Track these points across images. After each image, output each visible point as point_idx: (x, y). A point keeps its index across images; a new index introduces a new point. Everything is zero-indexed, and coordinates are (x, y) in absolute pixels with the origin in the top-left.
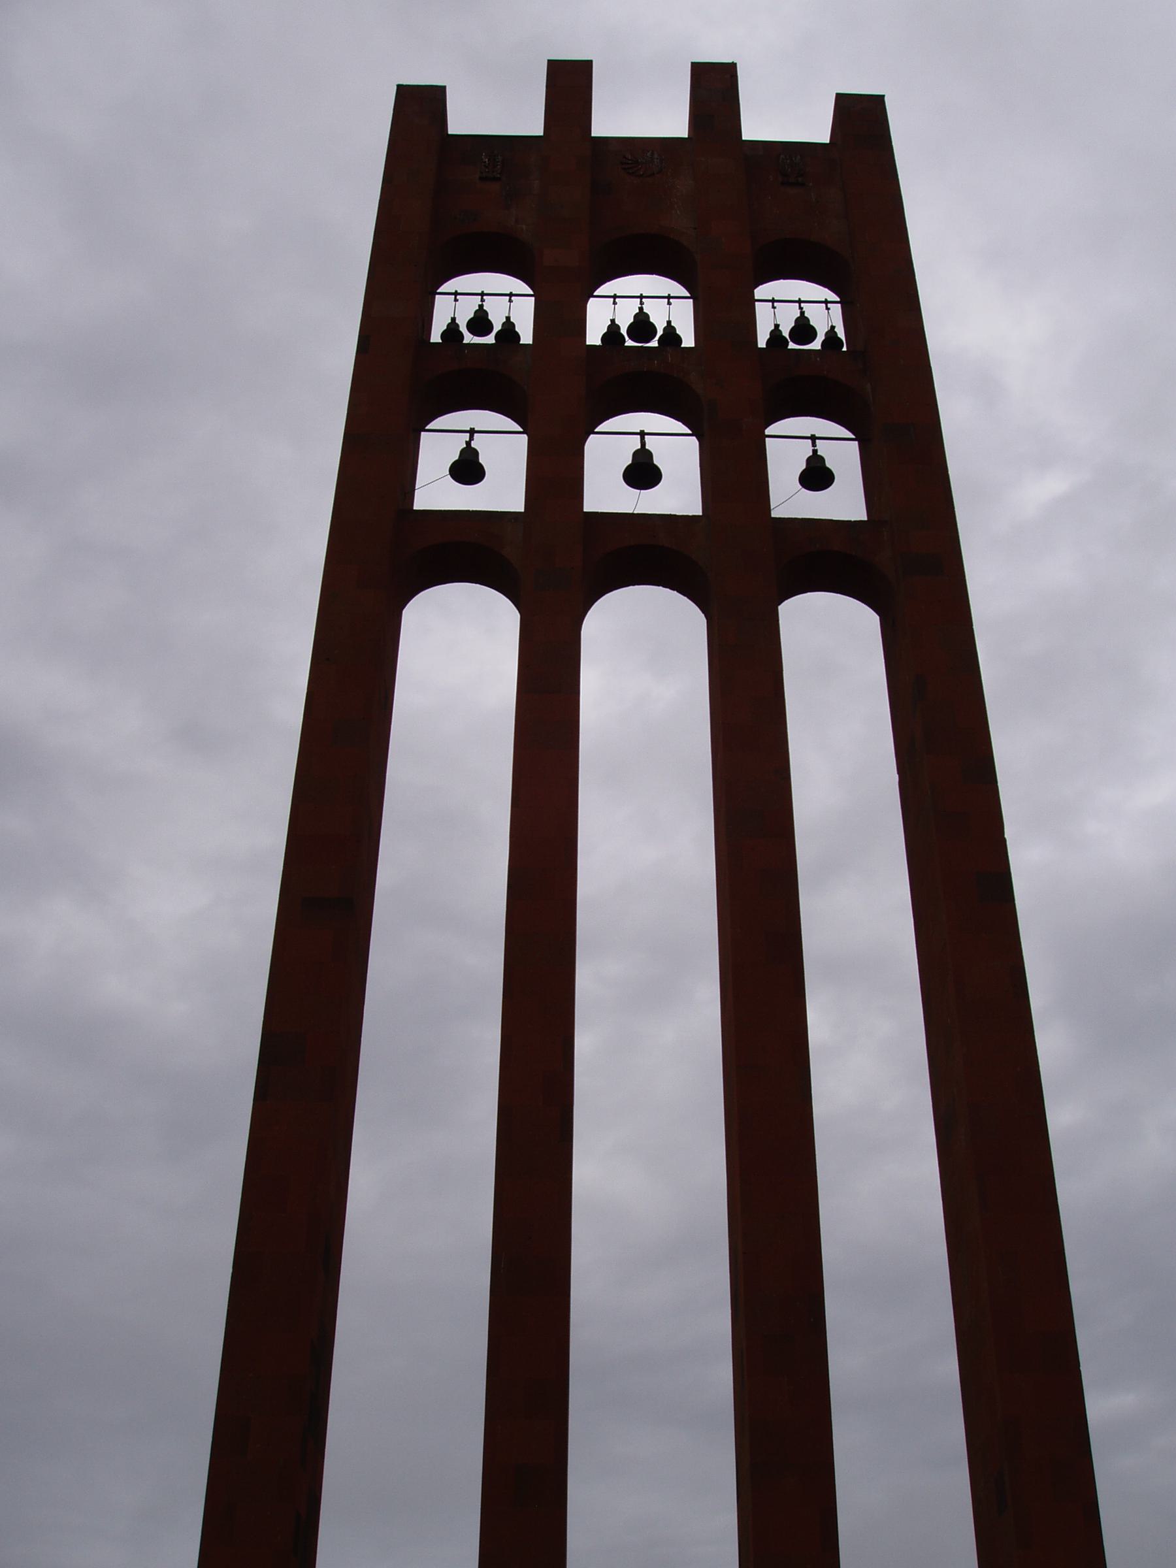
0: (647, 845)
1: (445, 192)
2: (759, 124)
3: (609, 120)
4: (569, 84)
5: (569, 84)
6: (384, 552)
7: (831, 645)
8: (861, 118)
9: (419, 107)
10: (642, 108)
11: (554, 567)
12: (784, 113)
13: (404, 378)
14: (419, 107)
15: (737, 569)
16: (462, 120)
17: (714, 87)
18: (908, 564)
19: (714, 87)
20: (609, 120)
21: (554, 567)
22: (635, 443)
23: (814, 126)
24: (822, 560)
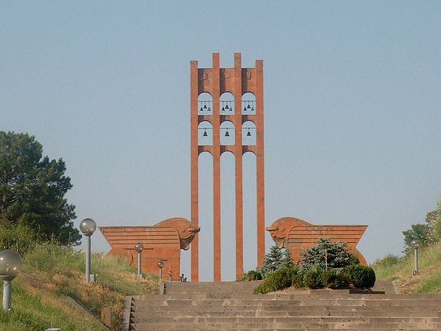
4: (216, 57)
5: (216, 57)
8: (260, 64)
10: (227, 63)
17: (238, 57)
19: (238, 57)
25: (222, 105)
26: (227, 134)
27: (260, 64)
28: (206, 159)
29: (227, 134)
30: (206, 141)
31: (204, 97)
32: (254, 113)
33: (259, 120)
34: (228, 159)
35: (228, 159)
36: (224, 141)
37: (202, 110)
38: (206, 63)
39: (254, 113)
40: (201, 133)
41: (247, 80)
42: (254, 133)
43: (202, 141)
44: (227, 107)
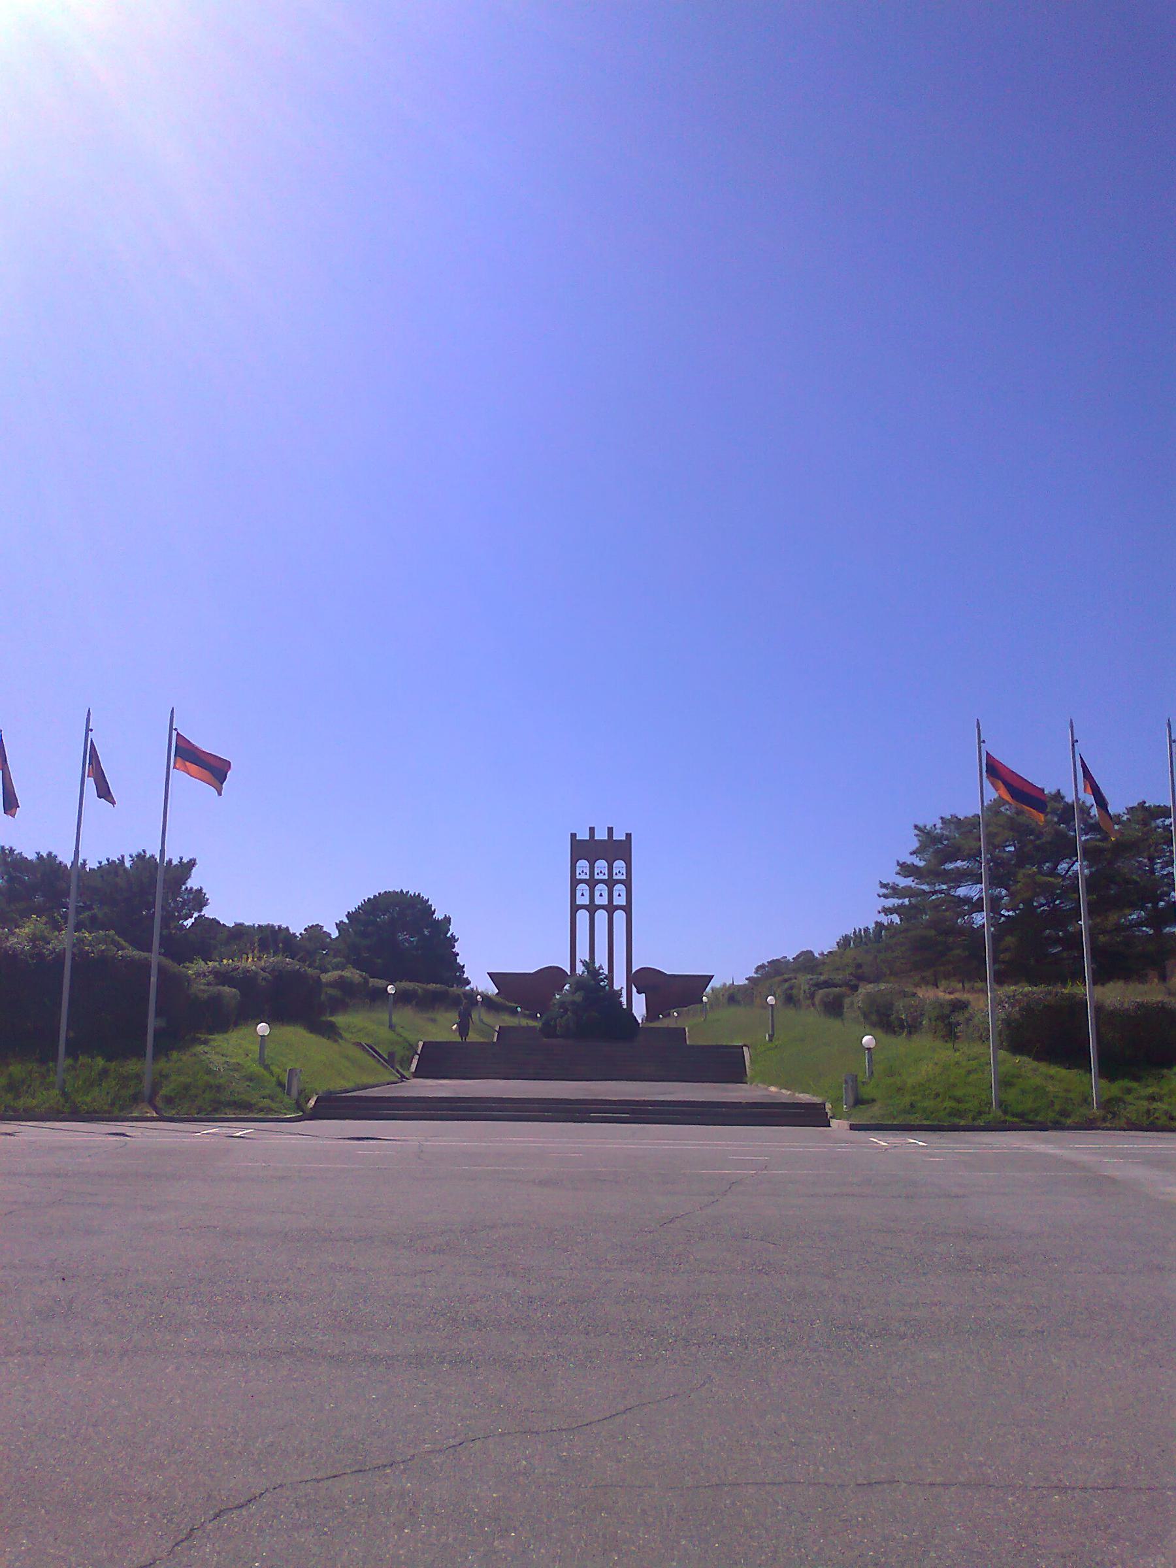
4: (592, 830)
5: (592, 830)
6: (575, 908)
7: (619, 916)
8: (629, 836)
9: (573, 836)
10: (601, 835)
11: (592, 909)
12: (619, 836)
13: (575, 883)
14: (573, 836)
15: (611, 909)
17: (610, 830)
18: (627, 909)
19: (610, 830)
21: (592, 909)
27: (629, 836)
28: (583, 916)
30: (583, 900)
31: (583, 864)
32: (624, 877)
33: (627, 883)
34: (601, 916)
35: (601, 916)
39: (624, 877)
41: (619, 849)
42: (624, 894)
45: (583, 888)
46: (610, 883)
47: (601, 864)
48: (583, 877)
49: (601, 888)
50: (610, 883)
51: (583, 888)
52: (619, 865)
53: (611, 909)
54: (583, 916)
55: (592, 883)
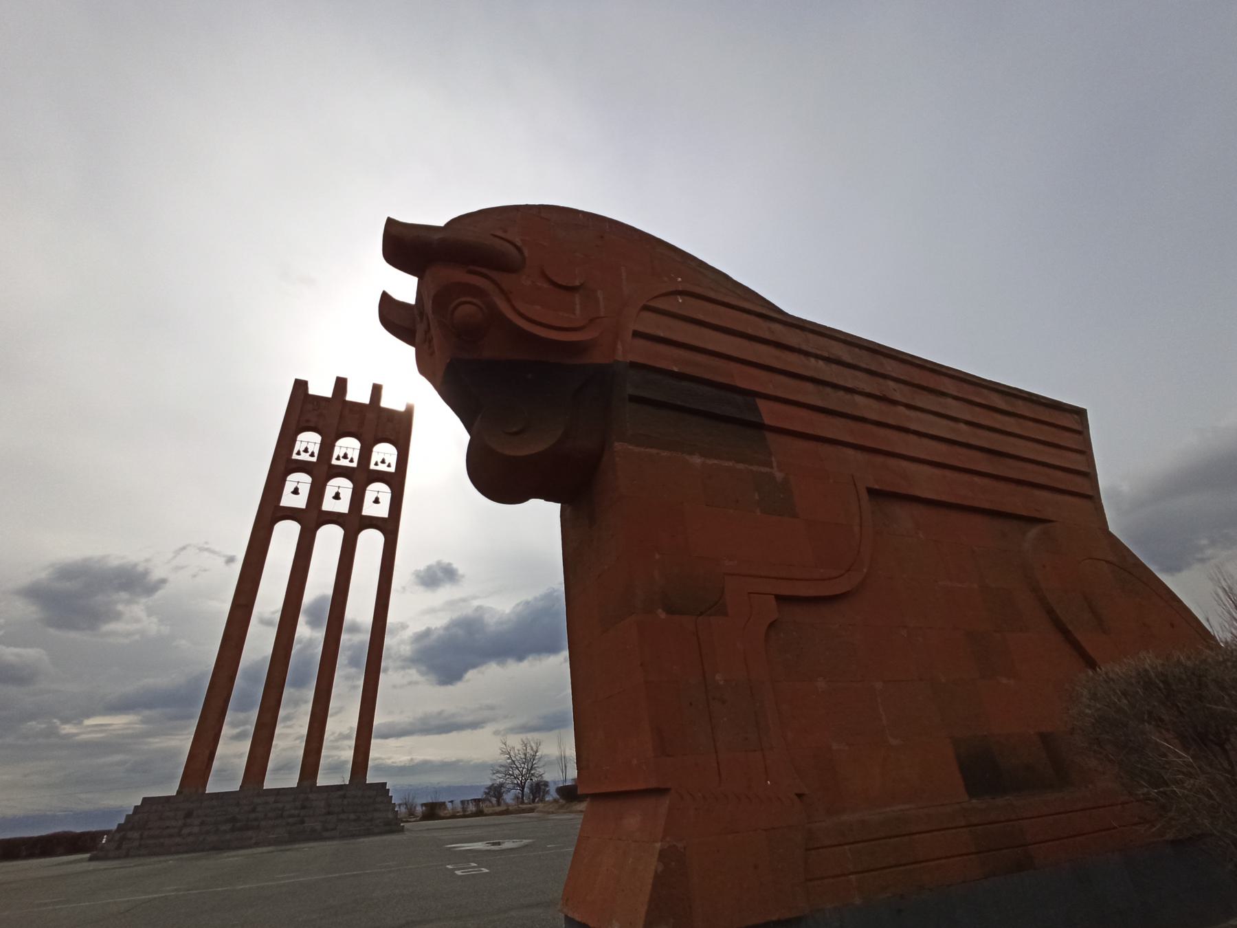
0: (320, 581)
1: (304, 410)
2: (386, 403)
3: (352, 396)
4: (341, 384)
5: (341, 384)
6: (270, 512)
7: (370, 543)
10: (358, 394)
13: (283, 464)
15: (353, 523)
16: (313, 390)
17: (377, 390)
18: (389, 527)
19: (377, 390)
20: (352, 396)
21: (312, 518)
22: (336, 490)
23: (400, 407)
24: (373, 523)
25: (338, 451)
26: (337, 497)
28: (286, 535)
29: (337, 497)
31: (308, 443)
32: (392, 469)
33: (396, 481)
35: (329, 539)
36: (329, 505)
37: (298, 453)
38: (322, 388)
39: (392, 469)
40: (289, 487)
43: (288, 500)
44: (345, 457)
45: (300, 482)
46: (362, 476)
47: (348, 448)
48: (305, 457)
49: (343, 485)
50: (362, 476)
51: (300, 482)
52: (384, 455)
53: (353, 523)
54: (286, 535)
55: (322, 471)
